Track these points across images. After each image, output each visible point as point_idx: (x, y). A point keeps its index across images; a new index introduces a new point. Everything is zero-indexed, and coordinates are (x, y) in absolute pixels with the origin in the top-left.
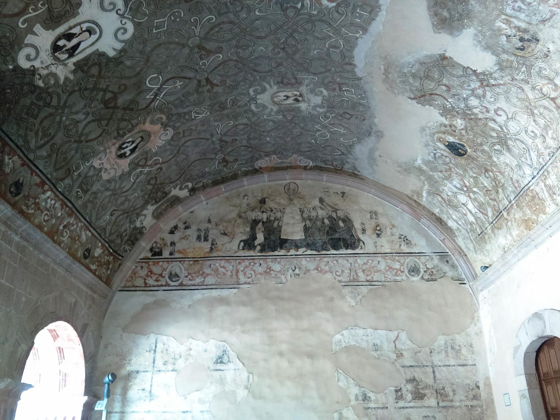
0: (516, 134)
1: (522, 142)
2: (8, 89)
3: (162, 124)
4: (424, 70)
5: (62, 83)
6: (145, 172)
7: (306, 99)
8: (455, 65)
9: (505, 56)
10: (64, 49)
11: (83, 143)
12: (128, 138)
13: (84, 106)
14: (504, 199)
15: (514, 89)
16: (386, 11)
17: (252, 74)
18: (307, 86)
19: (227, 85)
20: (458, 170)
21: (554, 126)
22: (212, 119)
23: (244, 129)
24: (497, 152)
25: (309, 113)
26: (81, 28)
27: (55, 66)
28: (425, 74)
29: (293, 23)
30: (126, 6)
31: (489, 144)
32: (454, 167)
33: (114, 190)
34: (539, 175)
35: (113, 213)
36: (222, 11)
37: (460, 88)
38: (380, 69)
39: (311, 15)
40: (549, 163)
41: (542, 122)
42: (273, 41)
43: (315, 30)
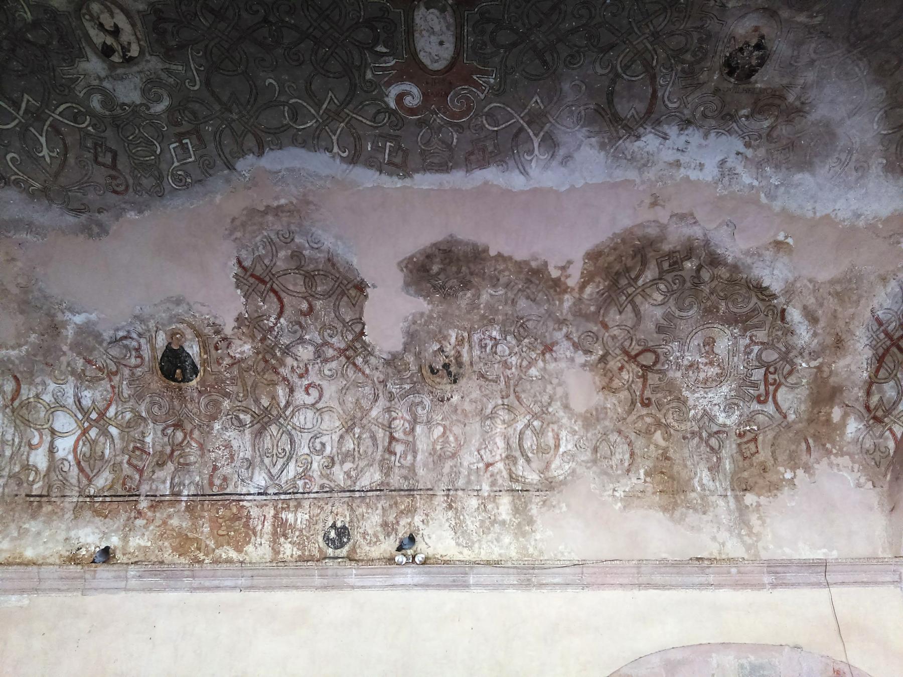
0: (298, 428)
1: (292, 442)
4: (321, 267)
7: (120, 71)
8: (357, 304)
9: (410, 358)
14: (164, 482)
15: (367, 390)
16: (404, 187)
18: (168, 71)
20: (124, 386)
21: (362, 464)
24: (235, 422)
28: (315, 271)
31: (239, 404)
32: (127, 376)
34: (276, 497)
37: (319, 327)
38: (277, 198)
40: (312, 495)
41: (349, 445)
43: (329, 77)
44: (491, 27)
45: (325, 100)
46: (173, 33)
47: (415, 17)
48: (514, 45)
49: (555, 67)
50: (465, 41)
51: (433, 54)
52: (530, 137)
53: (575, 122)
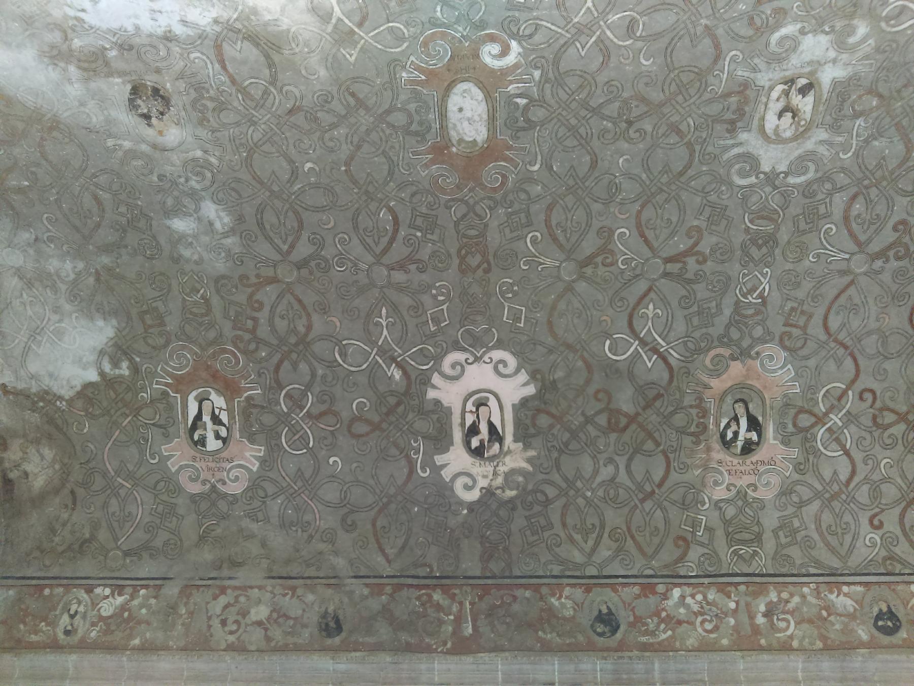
2: (487, 531)
3: (734, 359)
5: (531, 469)
6: (840, 424)
7: (807, 69)
10: (486, 444)
11: (657, 491)
12: (717, 422)
13: (593, 458)
17: (692, 178)
18: (755, 70)
19: (704, 225)
22: (789, 266)
23: (868, 202)
25: (867, 57)
26: (471, 412)
27: (501, 464)
29: (564, 109)
30: (464, 350)
33: (817, 495)
35: (876, 522)
36: (524, 220)
39: (545, 79)
42: (606, 142)
43: (581, 71)
44: (414, 127)
45: (591, 45)
46: (728, 109)
47: (487, 133)
48: (388, 112)
49: (341, 92)
50: (437, 113)
51: (469, 98)
52: (347, 18)
53: (299, 36)
